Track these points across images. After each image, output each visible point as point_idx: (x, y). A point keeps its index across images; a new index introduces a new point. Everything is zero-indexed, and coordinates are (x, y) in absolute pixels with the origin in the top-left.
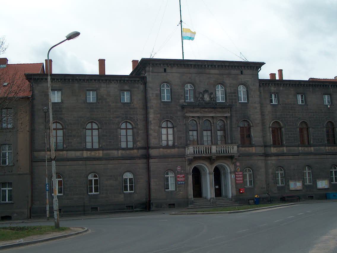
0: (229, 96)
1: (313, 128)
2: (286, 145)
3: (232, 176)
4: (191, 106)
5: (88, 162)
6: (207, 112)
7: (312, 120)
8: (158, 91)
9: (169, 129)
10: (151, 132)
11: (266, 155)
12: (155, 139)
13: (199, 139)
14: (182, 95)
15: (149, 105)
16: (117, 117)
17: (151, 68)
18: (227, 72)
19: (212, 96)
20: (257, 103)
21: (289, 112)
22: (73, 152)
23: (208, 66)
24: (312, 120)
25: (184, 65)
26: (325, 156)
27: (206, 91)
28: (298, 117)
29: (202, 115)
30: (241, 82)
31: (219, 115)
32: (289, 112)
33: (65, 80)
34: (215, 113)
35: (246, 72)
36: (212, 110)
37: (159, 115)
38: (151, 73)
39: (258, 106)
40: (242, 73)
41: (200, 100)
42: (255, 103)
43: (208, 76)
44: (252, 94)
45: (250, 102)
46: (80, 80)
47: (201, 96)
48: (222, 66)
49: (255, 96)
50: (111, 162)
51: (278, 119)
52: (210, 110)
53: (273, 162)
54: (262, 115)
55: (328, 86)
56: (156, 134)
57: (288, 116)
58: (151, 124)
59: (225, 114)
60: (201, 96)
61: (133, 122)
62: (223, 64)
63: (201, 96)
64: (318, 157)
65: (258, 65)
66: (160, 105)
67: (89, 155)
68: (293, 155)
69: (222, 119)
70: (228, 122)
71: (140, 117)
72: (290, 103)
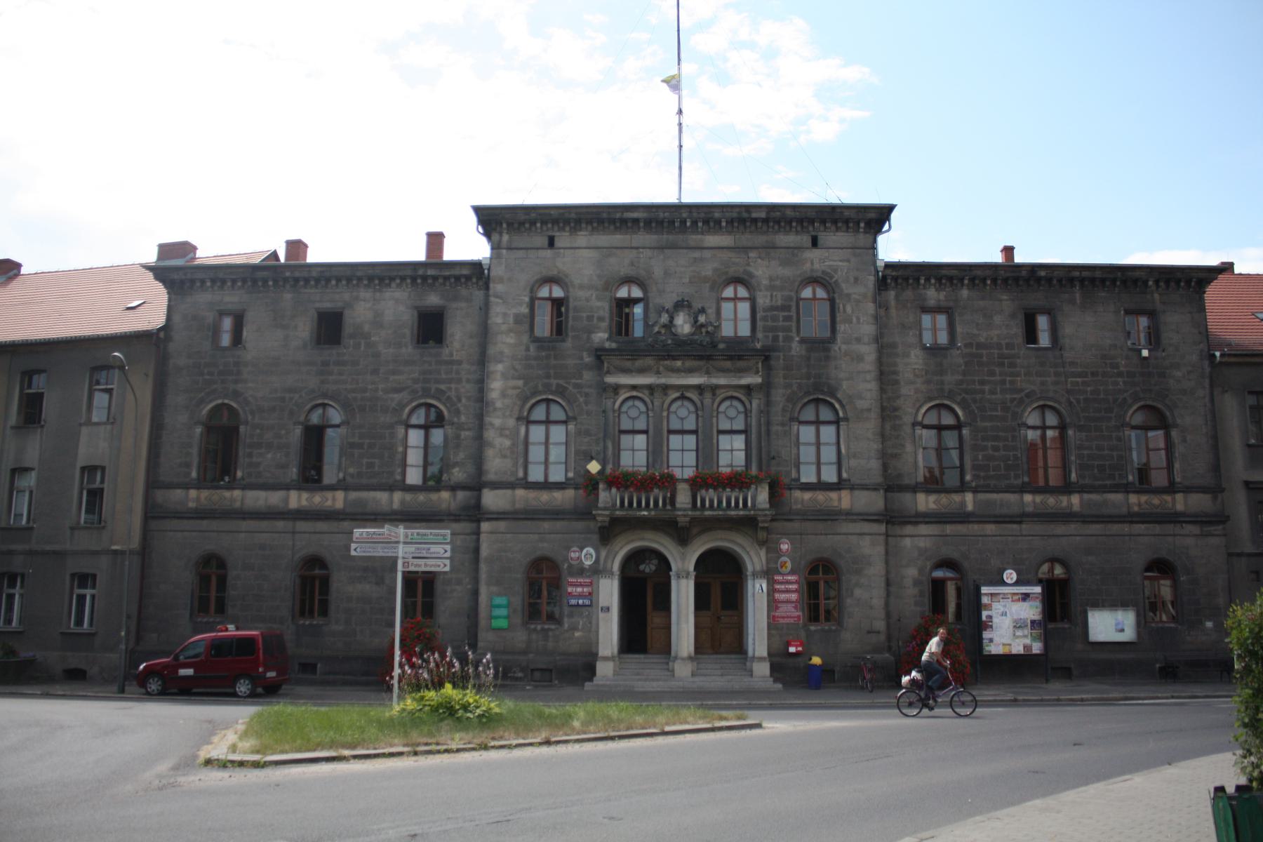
0: (765, 319)
1: (1080, 428)
2: (974, 484)
3: (758, 586)
5: (302, 526)
7: (1078, 401)
10: (490, 434)
11: (893, 519)
12: (504, 457)
15: (492, 351)
17: (506, 238)
18: (760, 239)
19: (702, 319)
20: (866, 339)
21: (992, 373)
22: (262, 494)
23: (695, 223)
24: (1078, 401)
26: (1126, 528)
28: (1021, 390)
29: (663, 381)
30: (812, 270)
31: (722, 381)
32: (992, 373)
33: (255, 281)
34: (708, 373)
35: (833, 237)
36: (701, 363)
37: (520, 383)
38: (504, 251)
39: (869, 352)
40: (815, 242)
41: (659, 332)
42: (858, 340)
43: (697, 254)
44: (849, 309)
45: (839, 337)
46: (297, 280)
49: (858, 319)
51: (949, 398)
52: (689, 363)
53: (922, 543)
54: (886, 377)
55: (1145, 283)
56: (507, 443)
57: (987, 388)
58: (495, 409)
60: (664, 318)
62: (745, 215)
64: (1095, 528)
65: (875, 218)
66: (528, 349)
67: (304, 503)
68: (1000, 520)
69: (735, 394)
72: (995, 340)
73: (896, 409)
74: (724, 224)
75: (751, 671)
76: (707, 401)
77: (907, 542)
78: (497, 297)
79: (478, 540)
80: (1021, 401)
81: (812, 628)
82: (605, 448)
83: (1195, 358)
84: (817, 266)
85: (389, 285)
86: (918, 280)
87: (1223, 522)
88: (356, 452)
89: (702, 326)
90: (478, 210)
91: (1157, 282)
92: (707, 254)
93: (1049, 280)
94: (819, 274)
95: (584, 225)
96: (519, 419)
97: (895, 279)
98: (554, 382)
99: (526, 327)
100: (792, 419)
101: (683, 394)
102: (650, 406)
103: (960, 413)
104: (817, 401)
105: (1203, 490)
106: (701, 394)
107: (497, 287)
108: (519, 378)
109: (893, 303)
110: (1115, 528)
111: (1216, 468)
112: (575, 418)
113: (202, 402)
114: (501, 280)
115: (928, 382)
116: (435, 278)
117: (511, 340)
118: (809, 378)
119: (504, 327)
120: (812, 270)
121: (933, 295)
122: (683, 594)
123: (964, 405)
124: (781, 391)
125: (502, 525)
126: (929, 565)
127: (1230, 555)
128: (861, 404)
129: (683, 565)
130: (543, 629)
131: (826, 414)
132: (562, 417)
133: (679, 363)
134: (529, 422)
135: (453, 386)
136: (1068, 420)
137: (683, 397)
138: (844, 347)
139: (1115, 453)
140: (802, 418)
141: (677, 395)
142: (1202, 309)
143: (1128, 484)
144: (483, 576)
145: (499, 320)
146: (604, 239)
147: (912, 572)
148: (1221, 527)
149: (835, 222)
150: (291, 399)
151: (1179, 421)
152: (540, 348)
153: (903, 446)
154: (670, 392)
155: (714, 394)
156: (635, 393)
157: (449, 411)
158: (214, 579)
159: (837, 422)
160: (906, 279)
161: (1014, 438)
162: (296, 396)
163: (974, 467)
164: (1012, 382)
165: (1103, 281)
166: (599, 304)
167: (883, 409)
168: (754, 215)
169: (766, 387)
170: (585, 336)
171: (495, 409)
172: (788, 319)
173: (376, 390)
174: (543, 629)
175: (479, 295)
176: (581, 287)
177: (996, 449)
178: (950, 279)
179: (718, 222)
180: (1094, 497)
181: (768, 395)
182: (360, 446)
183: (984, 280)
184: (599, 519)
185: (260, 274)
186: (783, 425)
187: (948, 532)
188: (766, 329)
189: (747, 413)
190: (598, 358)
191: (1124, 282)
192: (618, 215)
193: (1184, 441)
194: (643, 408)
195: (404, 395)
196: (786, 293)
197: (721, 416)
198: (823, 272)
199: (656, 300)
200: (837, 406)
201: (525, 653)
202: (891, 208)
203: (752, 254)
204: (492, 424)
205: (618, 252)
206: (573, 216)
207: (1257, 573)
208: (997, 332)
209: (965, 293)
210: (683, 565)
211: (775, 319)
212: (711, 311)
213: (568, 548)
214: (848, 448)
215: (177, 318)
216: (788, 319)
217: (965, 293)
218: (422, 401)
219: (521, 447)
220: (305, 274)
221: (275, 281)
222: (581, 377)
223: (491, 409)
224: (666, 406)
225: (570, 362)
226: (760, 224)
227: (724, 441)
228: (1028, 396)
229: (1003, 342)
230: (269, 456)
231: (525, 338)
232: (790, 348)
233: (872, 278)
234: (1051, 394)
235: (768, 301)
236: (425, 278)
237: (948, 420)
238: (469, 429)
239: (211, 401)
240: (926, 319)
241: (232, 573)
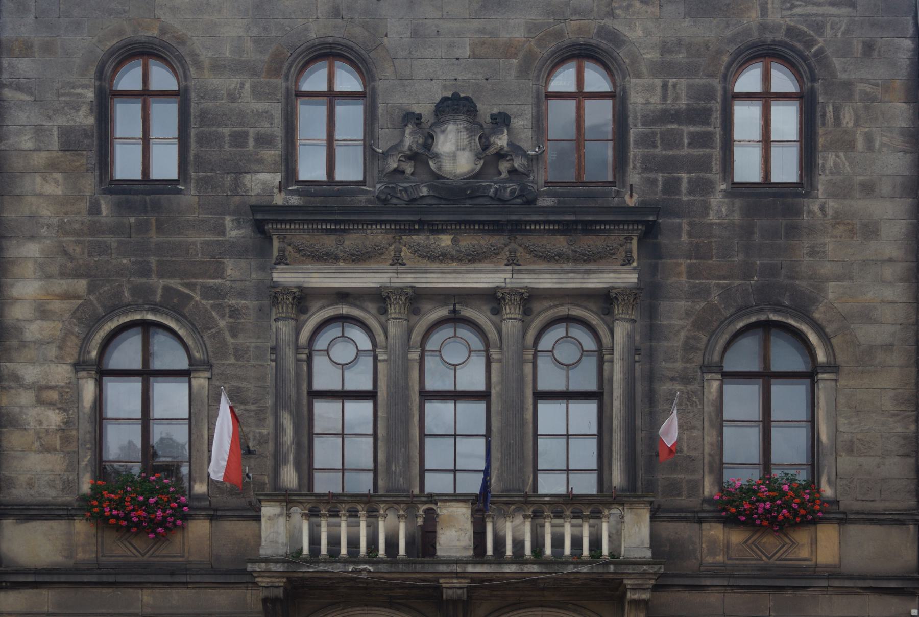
0: (646, 140)
4: (329, 213)
14: (264, 141)
19: (502, 141)
20: (886, 188)
27: (456, 106)
29: (407, 279)
30: (763, 27)
31: (546, 281)
34: (512, 262)
36: (498, 240)
41: (398, 171)
42: (868, 189)
44: (848, 120)
45: (822, 181)
47: (408, 141)
49: (869, 139)
52: (468, 242)
60: (409, 140)
63: (408, 141)
66: (95, 209)
70: (621, 330)
76: (511, 325)
89: (500, 156)
94: (780, 36)
99: (90, 157)
100: (707, 368)
101: (456, 308)
104: (766, 327)
106: (496, 311)
108: (78, 276)
118: (747, 277)
120: (763, 27)
124: (682, 304)
131: (786, 357)
133: (445, 241)
137: (455, 319)
138: (832, 204)
140: (730, 366)
141: (442, 312)
152: (122, 208)
154: (426, 306)
155: (527, 312)
156: (344, 310)
166: (260, 106)
169: (647, 298)
170: (228, 179)
172: (702, 140)
181: (652, 313)
186: (685, 379)
188: (649, 165)
189: (602, 355)
190: (260, 227)
194: (365, 343)
196: (700, 81)
198: (790, 31)
199: (394, 98)
211: (671, 141)
212: (522, 124)
216: (702, 140)
222: (219, 272)
224: (416, 337)
225: (197, 239)
231: (89, 184)
232: (706, 208)
235: (656, 99)
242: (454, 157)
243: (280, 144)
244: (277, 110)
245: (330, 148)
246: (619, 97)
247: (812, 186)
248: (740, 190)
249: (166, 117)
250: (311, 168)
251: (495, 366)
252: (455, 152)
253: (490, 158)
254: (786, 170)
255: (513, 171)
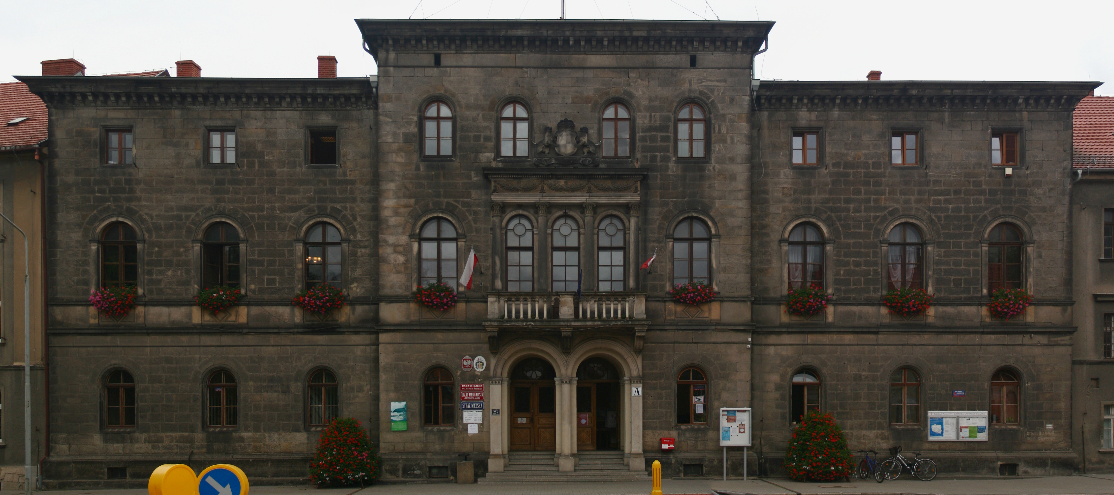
0: (643, 139)
2: (835, 298)
3: (634, 390)
6: (561, 190)
7: (939, 218)
8: (413, 125)
9: (444, 245)
10: (387, 251)
11: (757, 329)
12: (398, 272)
13: (536, 275)
14: (487, 139)
15: (383, 170)
16: (295, 209)
17: (392, 55)
18: (641, 59)
19: (585, 139)
20: (739, 160)
22: (165, 310)
23: (577, 42)
25: (497, 39)
26: (977, 339)
27: (566, 124)
28: (886, 208)
29: (547, 199)
30: (690, 91)
31: (603, 200)
32: (858, 192)
34: (589, 191)
35: (709, 58)
36: (583, 182)
37: (412, 201)
38: (391, 69)
39: (741, 171)
40: (693, 63)
41: (543, 152)
42: (732, 160)
43: (579, 74)
44: (724, 130)
45: (714, 156)
46: (184, 96)
47: (547, 139)
48: (624, 40)
49: (732, 139)
50: (273, 339)
51: (815, 216)
52: (571, 183)
53: (785, 351)
54: (757, 195)
55: (1015, 100)
56: (401, 259)
57: (852, 206)
59: (620, 196)
61: (341, 223)
62: (627, 34)
63: (547, 139)
65: (753, 35)
66: (418, 168)
68: (856, 331)
69: (615, 213)
70: (633, 221)
71: (363, 207)
72: (862, 159)
73: (764, 227)
74: (606, 43)
75: (628, 465)
76: (588, 219)
77: (771, 350)
78: (386, 116)
79: (377, 351)
80: (884, 219)
81: (683, 427)
82: (494, 263)
83: (1057, 176)
84: (694, 87)
85: (279, 104)
86: (790, 100)
87: (1070, 333)
88: (257, 269)
89: (584, 146)
90: (363, 24)
91: (1027, 100)
92: (590, 74)
93: (919, 99)
94: (697, 95)
95: (469, 43)
96: (411, 236)
97: (769, 99)
98: (444, 200)
100: (668, 236)
101: (566, 211)
102: (535, 224)
103: (825, 230)
104: (691, 219)
105: (1054, 303)
106: (583, 212)
107: (385, 106)
109: (765, 123)
110: (967, 339)
111: (1069, 282)
112: (464, 236)
113: (94, 220)
114: (389, 99)
115: (795, 201)
116: (325, 97)
117: (401, 159)
119: (395, 146)
120: (690, 91)
121: (805, 116)
122: (566, 397)
123: (829, 222)
124: (658, 209)
125: (398, 336)
126: (790, 371)
127: (1074, 363)
128: (732, 222)
129: (566, 369)
130: (439, 431)
131: (699, 230)
132: (454, 235)
133: (562, 183)
134: (421, 240)
135: (348, 205)
136: (928, 237)
137: (566, 216)
138: (717, 166)
139: (971, 269)
140: (676, 236)
141: (561, 213)
142: (1069, 127)
143: (982, 297)
144: (382, 386)
145: (389, 139)
146: (488, 58)
147: (775, 378)
148: (1067, 337)
149: (713, 41)
150: (188, 217)
151: (1036, 237)
153: (769, 262)
155: (595, 213)
156: (520, 212)
157: (345, 230)
158: (122, 393)
159: (708, 239)
160: (779, 99)
161: (875, 254)
162: (193, 214)
163: (837, 282)
164: (876, 201)
165: (973, 99)
166: (485, 124)
167: (752, 226)
168: (635, 34)
169: (643, 207)
171: (389, 227)
172: (666, 139)
173: (273, 209)
174: (439, 431)
175: (368, 114)
176: (468, 107)
177: (857, 264)
178: (822, 99)
179: (600, 41)
180: (949, 309)
181: (645, 213)
182: (260, 263)
183: (855, 100)
184: (489, 329)
185: (143, 89)
186: (659, 241)
187: (809, 341)
189: (625, 231)
190: (486, 177)
191: (994, 100)
192: (503, 33)
193: (1040, 256)
194: (529, 226)
195: (300, 214)
197: (602, 234)
198: (701, 93)
200: (710, 223)
201: (423, 452)
202: (768, 26)
203: (632, 75)
204: (386, 242)
205: (503, 70)
206: (458, 33)
207: (1097, 380)
208: (865, 151)
209: (836, 113)
210: (566, 369)
211: (653, 139)
212: (593, 132)
213: (461, 357)
214: (719, 263)
215: (60, 134)
216: (666, 139)
217: (836, 113)
218: (319, 220)
219: (414, 263)
220: (191, 90)
221: (162, 97)
222: (469, 196)
223: (385, 226)
224: (550, 224)
226: (640, 43)
227: (604, 257)
228: (891, 213)
229: (870, 162)
230: (170, 273)
231: (415, 157)
232: (667, 168)
233: (747, 98)
234: (913, 212)
235: (647, 121)
236: (315, 97)
237: (811, 236)
238: (365, 247)
239: (104, 220)
240: (797, 142)
241: (139, 387)
242: (565, 146)
243: (494, 140)
244: (492, 125)
245: (515, 139)
246: (632, 120)
247: (710, 159)
248: (680, 160)
249: (447, 127)
250: (506, 150)
251: (582, 236)
252: (565, 143)
253: (580, 146)
254: (699, 152)
255: (589, 152)
